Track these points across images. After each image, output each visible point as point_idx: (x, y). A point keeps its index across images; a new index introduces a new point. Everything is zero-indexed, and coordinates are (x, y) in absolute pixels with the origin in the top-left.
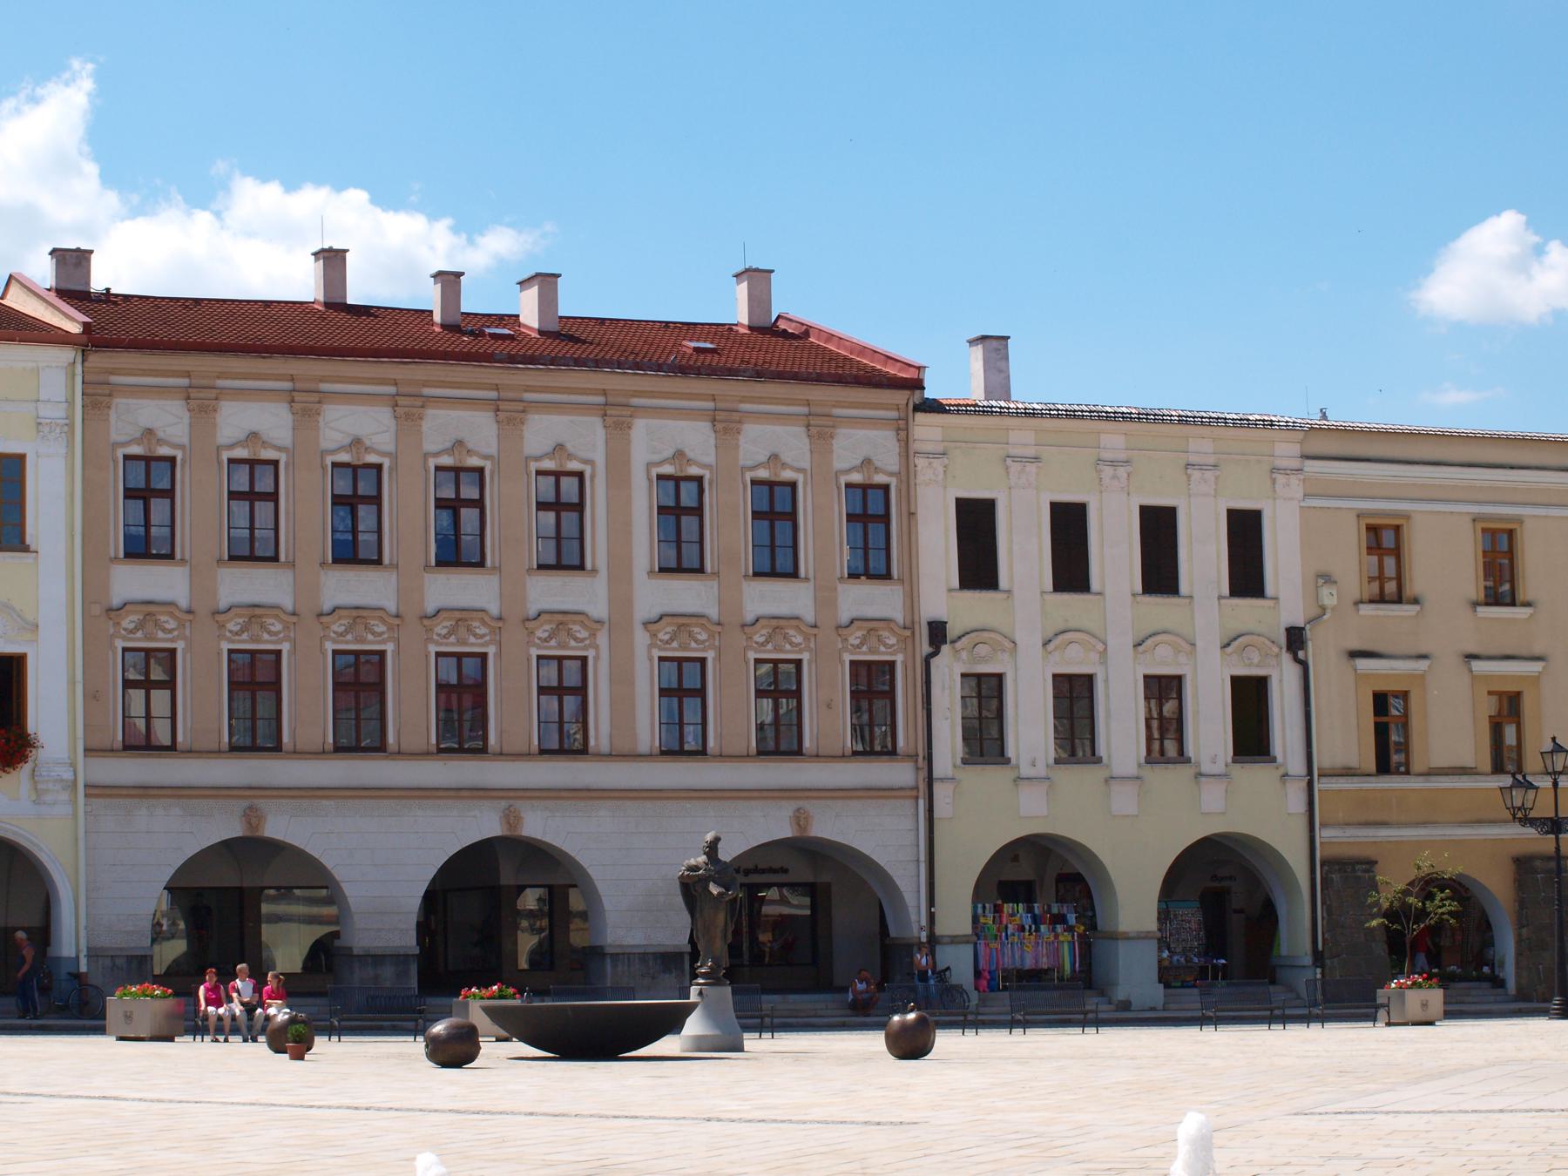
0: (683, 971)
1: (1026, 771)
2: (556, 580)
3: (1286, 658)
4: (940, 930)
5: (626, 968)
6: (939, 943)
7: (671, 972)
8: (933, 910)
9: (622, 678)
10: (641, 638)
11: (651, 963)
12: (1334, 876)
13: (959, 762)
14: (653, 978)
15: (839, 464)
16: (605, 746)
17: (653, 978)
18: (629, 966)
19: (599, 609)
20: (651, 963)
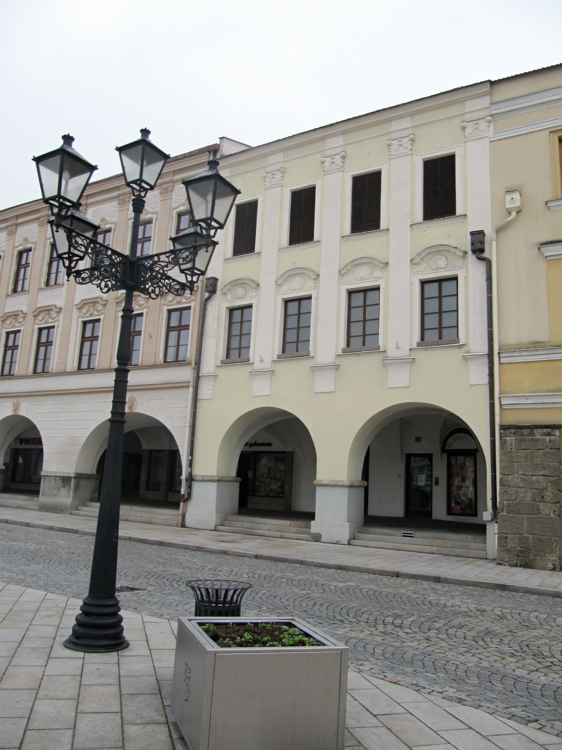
0: (70, 487)
1: (257, 366)
2: (49, 292)
3: (471, 257)
4: (198, 471)
5: (48, 484)
6: (196, 481)
7: (65, 488)
8: (190, 458)
9: (66, 335)
10: (76, 313)
11: (58, 482)
12: (508, 438)
13: (219, 364)
14: (58, 490)
15: (174, 205)
16: (54, 371)
17: (58, 490)
18: (49, 483)
19: (60, 303)
20: (58, 482)
